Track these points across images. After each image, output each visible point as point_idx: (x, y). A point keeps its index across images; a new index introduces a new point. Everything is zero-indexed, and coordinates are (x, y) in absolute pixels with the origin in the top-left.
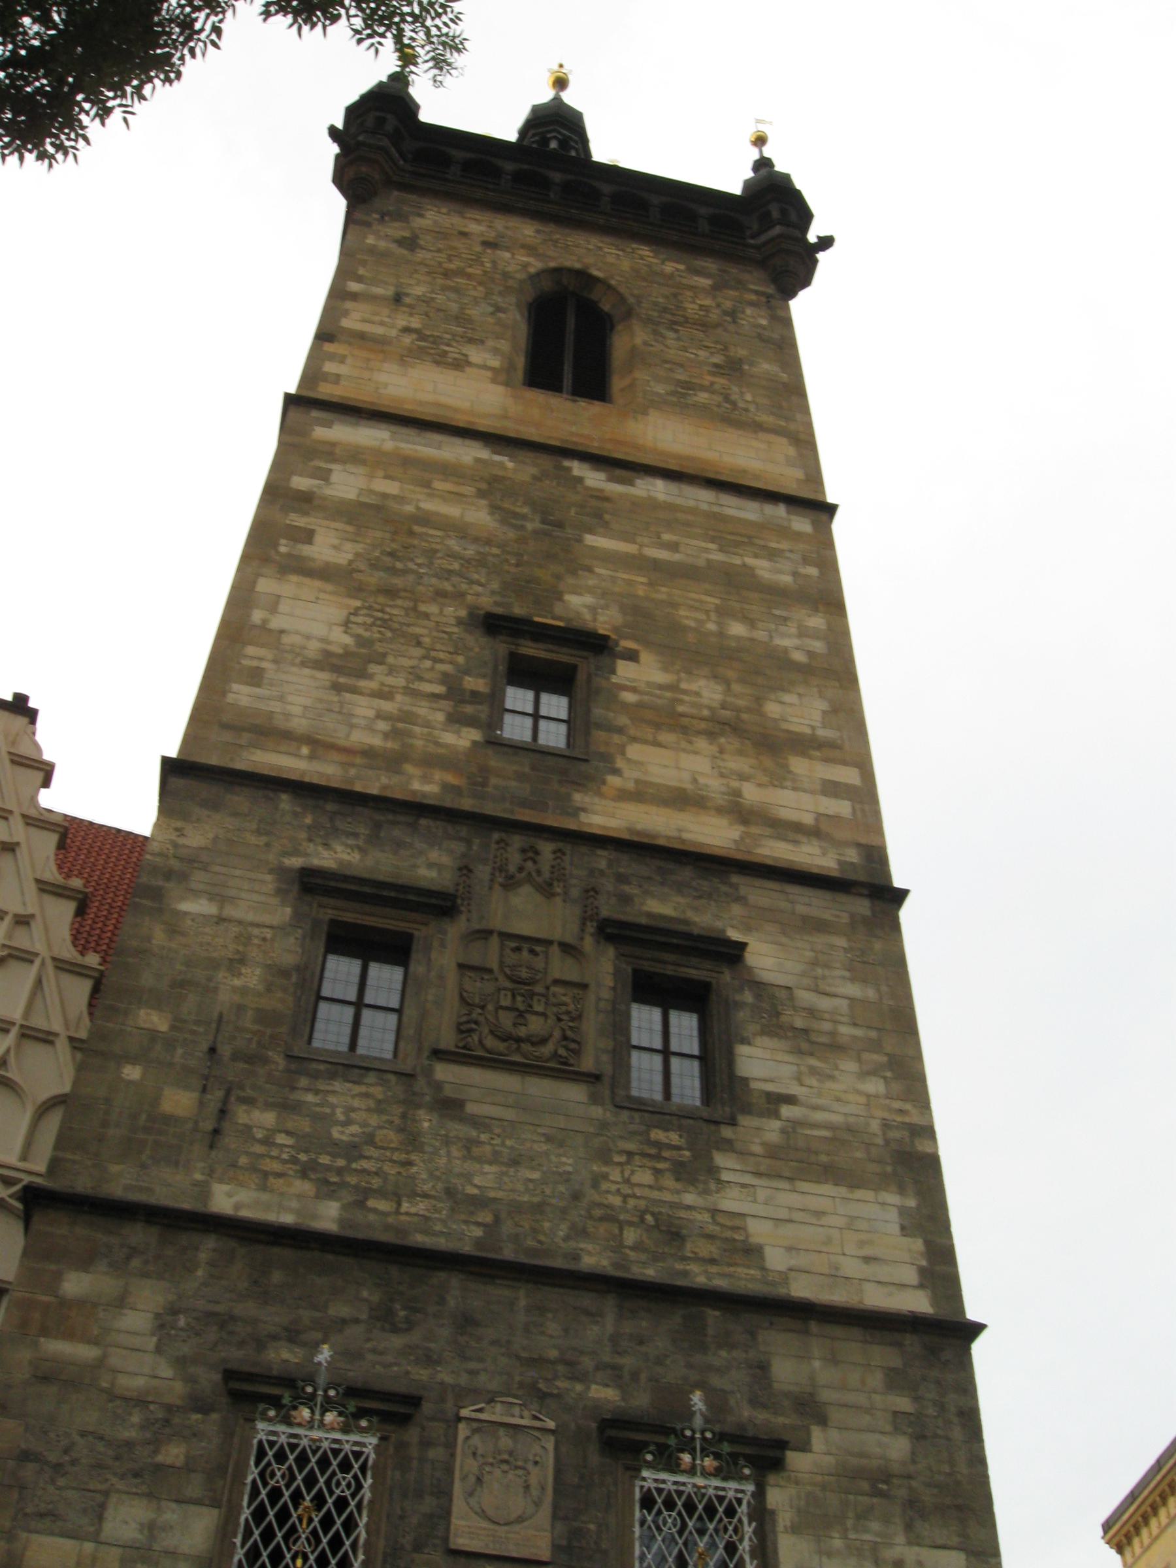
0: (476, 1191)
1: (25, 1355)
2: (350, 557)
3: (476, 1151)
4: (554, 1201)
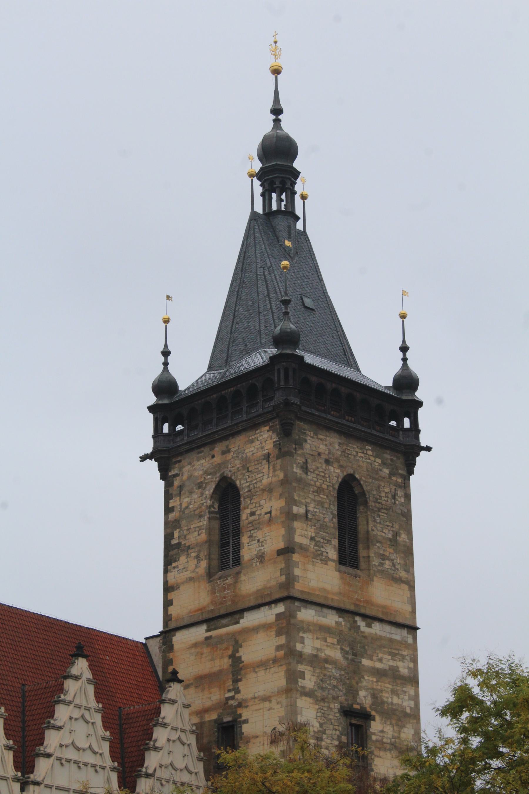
2: (313, 684)
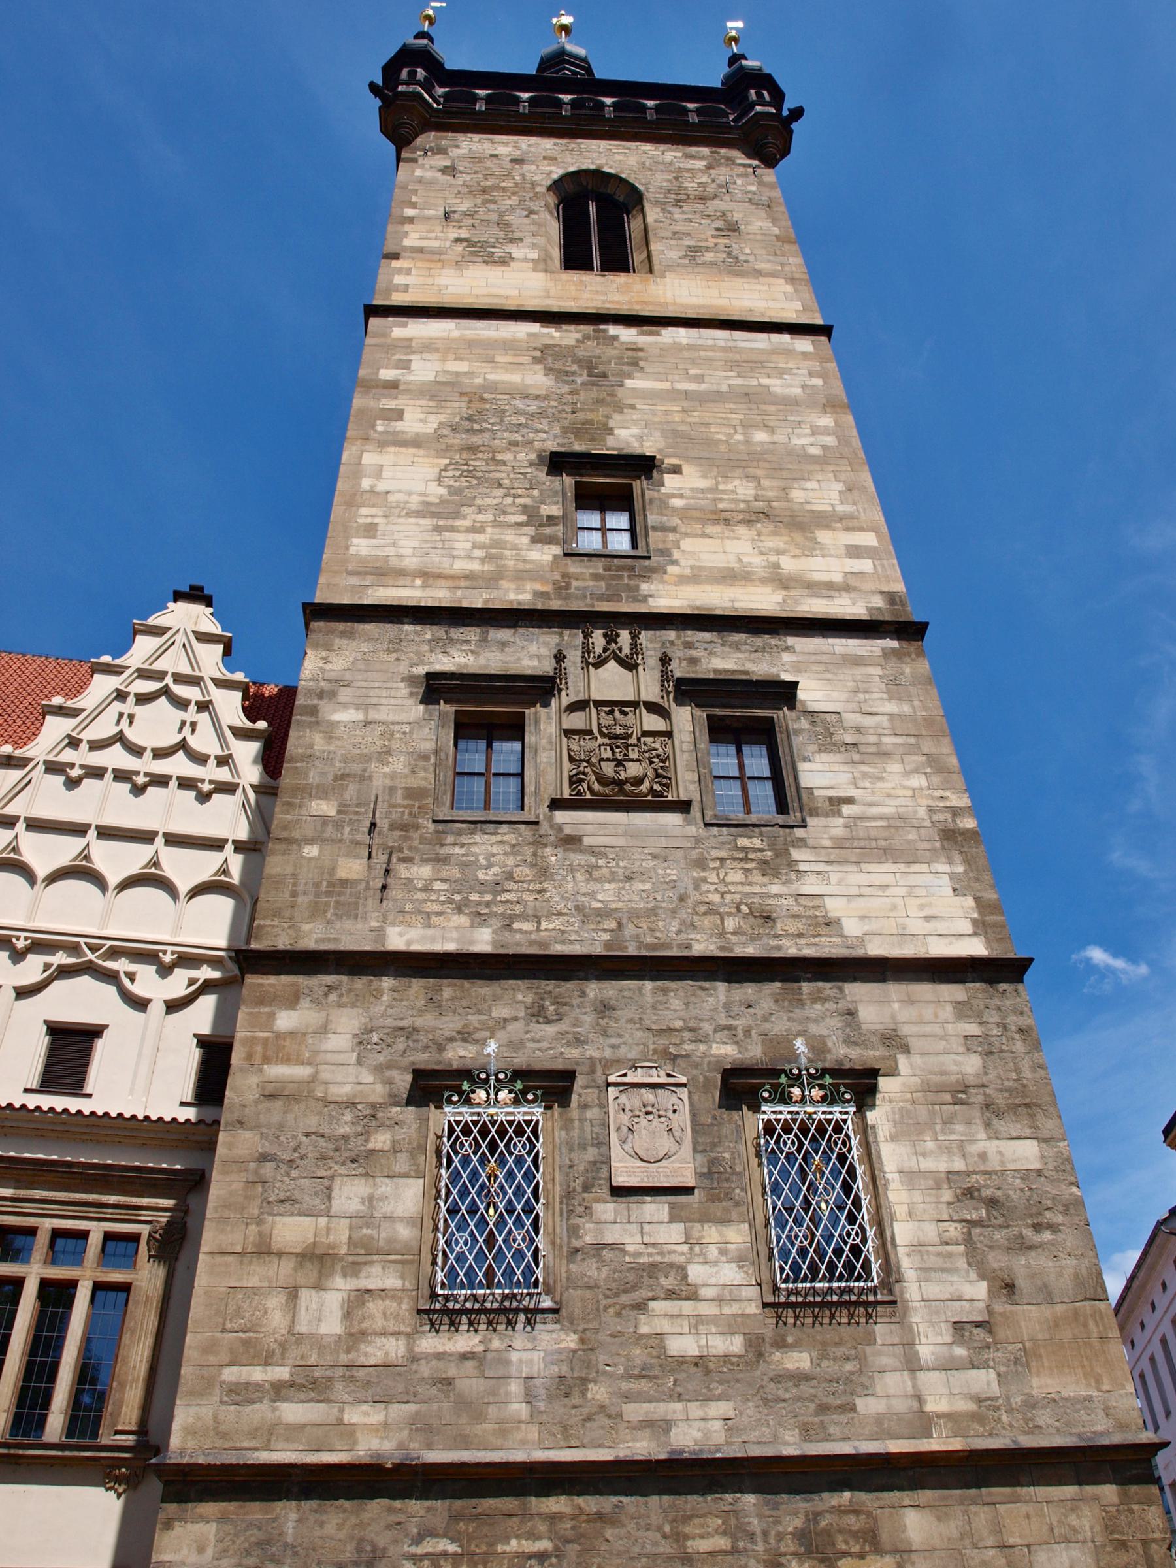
0: (600, 905)
1: (254, 1080)
2: (435, 426)
3: (596, 874)
4: (664, 905)
